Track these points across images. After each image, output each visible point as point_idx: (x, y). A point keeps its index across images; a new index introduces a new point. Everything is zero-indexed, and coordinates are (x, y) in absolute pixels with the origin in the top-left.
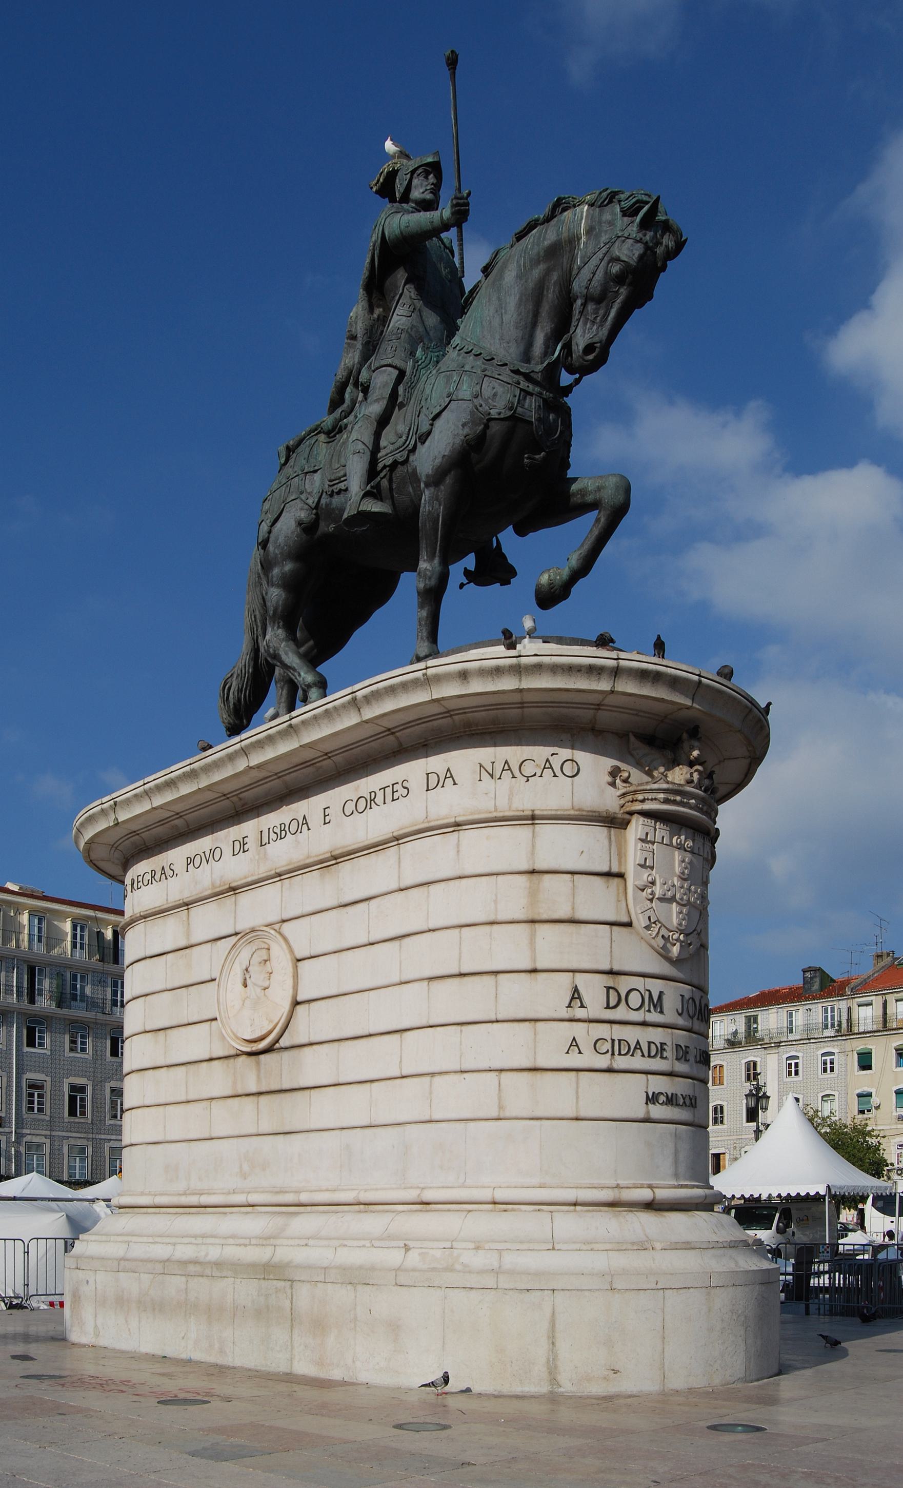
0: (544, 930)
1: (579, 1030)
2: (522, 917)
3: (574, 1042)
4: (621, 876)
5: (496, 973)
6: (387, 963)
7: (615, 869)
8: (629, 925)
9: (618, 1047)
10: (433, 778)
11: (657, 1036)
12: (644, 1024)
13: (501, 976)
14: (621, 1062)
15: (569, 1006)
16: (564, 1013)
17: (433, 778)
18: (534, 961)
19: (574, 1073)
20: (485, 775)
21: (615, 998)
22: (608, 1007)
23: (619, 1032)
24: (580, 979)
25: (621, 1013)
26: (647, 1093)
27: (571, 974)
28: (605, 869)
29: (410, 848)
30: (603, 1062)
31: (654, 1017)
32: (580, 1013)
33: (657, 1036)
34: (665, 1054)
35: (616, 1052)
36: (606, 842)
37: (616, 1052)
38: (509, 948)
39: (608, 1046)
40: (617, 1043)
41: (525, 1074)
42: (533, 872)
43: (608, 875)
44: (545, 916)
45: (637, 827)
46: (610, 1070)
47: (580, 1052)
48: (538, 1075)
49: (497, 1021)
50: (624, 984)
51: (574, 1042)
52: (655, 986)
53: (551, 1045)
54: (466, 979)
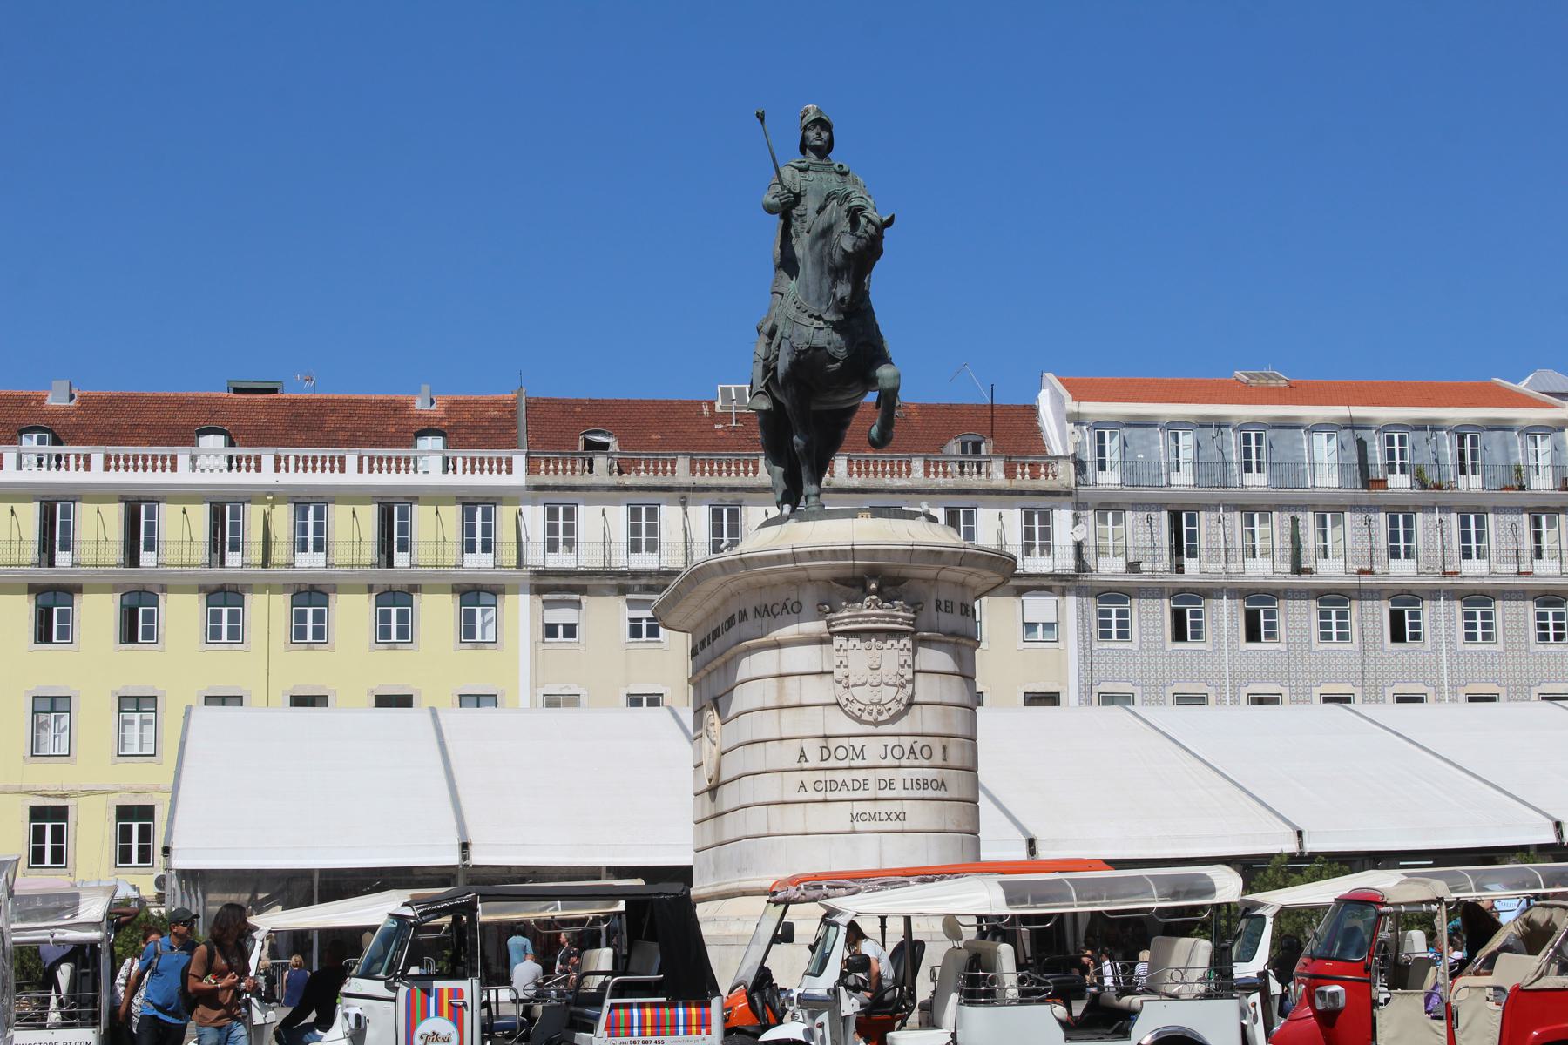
3: (802, 785)
8: (838, 704)
12: (850, 768)
16: (798, 766)
23: (830, 775)
30: (820, 796)
32: (806, 765)
33: (860, 775)
46: (826, 801)
50: (833, 744)
51: (802, 785)
52: (858, 743)
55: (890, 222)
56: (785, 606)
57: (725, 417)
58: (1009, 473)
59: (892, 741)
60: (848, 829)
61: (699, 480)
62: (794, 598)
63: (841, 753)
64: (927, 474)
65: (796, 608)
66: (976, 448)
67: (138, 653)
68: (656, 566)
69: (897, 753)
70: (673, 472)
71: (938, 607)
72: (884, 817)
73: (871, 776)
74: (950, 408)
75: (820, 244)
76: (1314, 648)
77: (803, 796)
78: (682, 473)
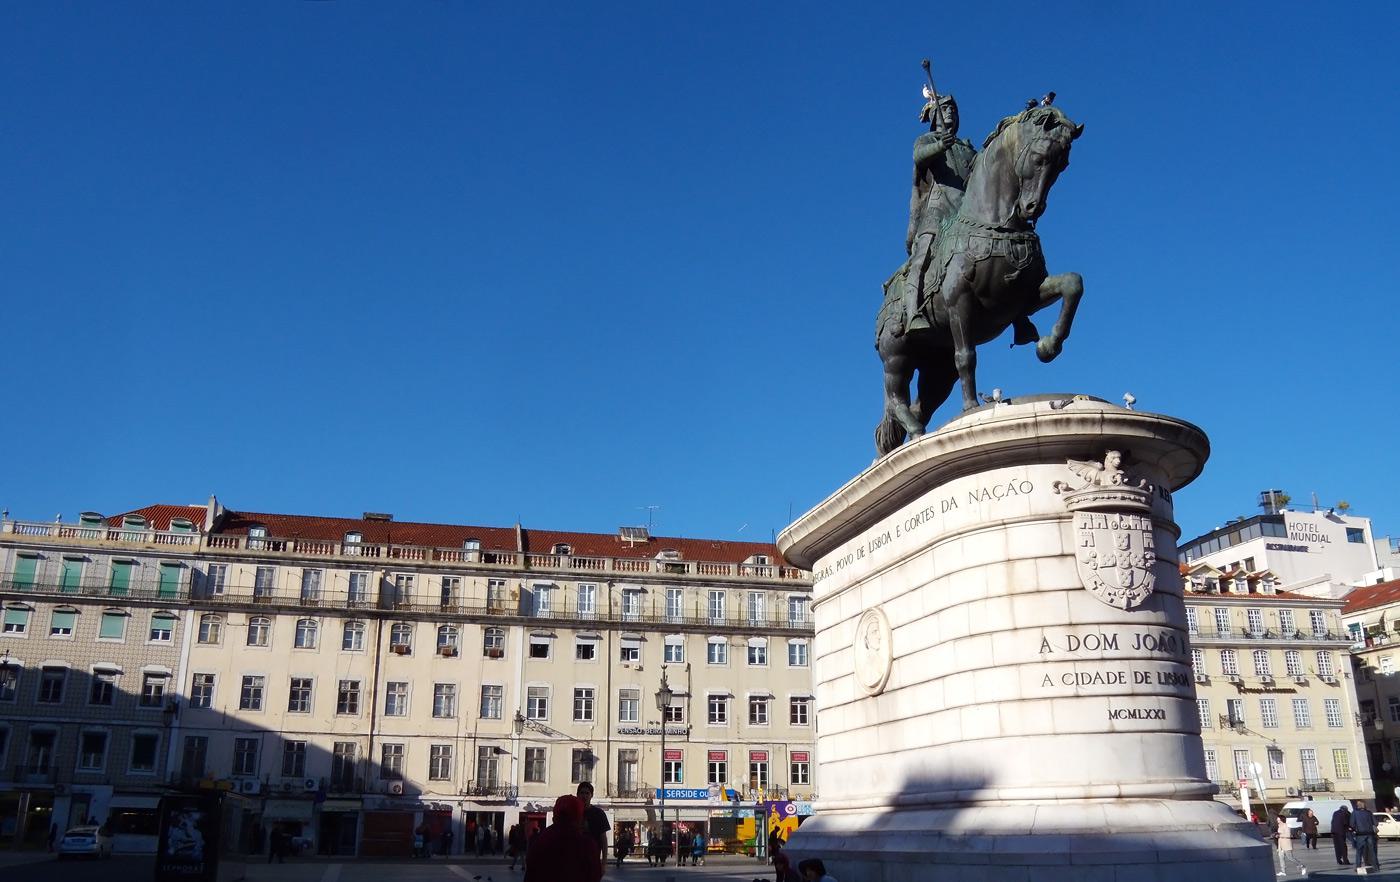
0: (1018, 600)
1: (1050, 669)
2: (1003, 591)
6: (930, 631)
8: (1083, 588)
9: (1079, 679)
10: (945, 504)
13: (995, 635)
14: (1082, 692)
16: (1039, 657)
17: (945, 504)
18: (1014, 622)
19: (1048, 701)
20: (972, 498)
21: (1075, 643)
23: (1080, 668)
24: (1049, 634)
27: (1040, 629)
28: (1059, 553)
29: (939, 550)
30: (1071, 690)
31: (1110, 653)
32: (1050, 657)
34: (1123, 680)
35: (1080, 683)
37: (1080, 683)
38: (997, 615)
40: (1080, 676)
41: (1015, 704)
43: (1063, 555)
44: (1019, 591)
45: (1079, 519)
46: (1078, 696)
48: (1024, 703)
49: (995, 667)
50: (1081, 632)
52: (1109, 631)
53: (1031, 682)
58: (782, 574)
59: (1143, 630)
60: (1106, 729)
61: (617, 572)
63: (1092, 642)
64: (739, 574)
65: (1025, 488)
66: (763, 561)
67: (303, 654)
70: (603, 567)
72: (1144, 714)
74: (743, 544)
75: (997, 163)
77: (1049, 691)
78: (608, 567)
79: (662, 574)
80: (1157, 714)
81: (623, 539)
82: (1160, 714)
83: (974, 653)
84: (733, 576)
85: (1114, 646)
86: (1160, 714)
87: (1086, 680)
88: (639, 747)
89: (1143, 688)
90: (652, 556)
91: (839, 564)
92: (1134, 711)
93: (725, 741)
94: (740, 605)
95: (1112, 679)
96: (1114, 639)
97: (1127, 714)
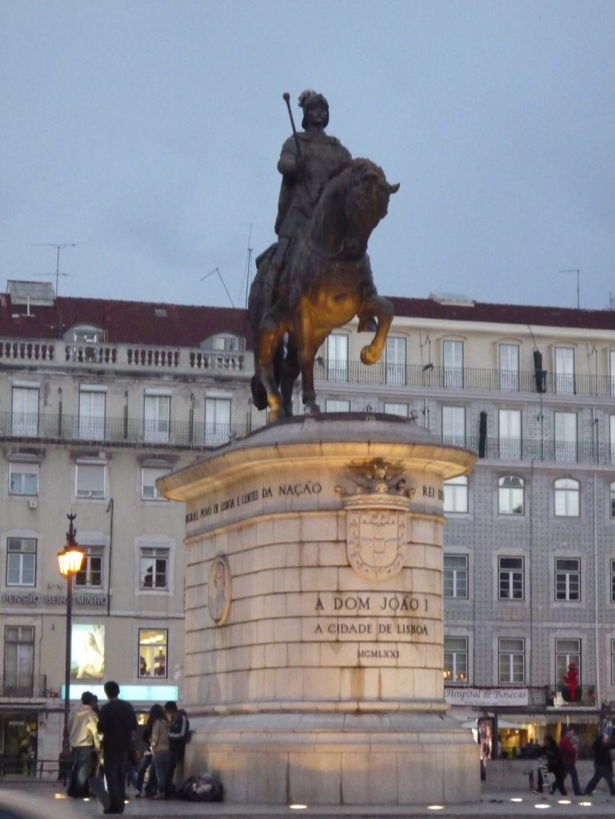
0: (306, 572)
2: (296, 564)
3: (319, 627)
4: (345, 541)
5: (285, 593)
7: (341, 538)
8: (349, 566)
11: (366, 622)
12: (358, 616)
15: (317, 608)
16: (315, 613)
18: (301, 586)
22: (336, 608)
23: (341, 621)
25: (343, 611)
26: (359, 652)
28: (334, 538)
30: (333, 637)
31: (363, 612)
32: (322, 613)
33: (366, 622)
36: (335, 525)
38: (290, 581)
39: (336, 628)
42: (301, 543)
43: (337, 542)
47: (321, 632)
50: (344, 597)
51: (319, 627)
52: (364, 597)
54: (277, 596)
55: (395, 189)
56: (307, 487)
57: (22, 308)
59: (389, 596)
60: (355, 663)
62: (315, 480)
63: (351, 603)
64: (192, 364)
65: (316, 488)
68: (36, 436)
69: (393, 604)
71: (425, 492)
72: (383, 654)
73: (373, 622)
74: (203, 307)
76: (494, 517)
79: (70, 363)
80: (393, 654)
81: (15, 301)
82: (396, 655)
83: (274, 606)
84: (184, 367)
85: (366, 607)
86: (395, 654)
87: (344, 629)
88: (37, 623)
89: (384, 637)
90: (57, 334)
91: (202, 512)
92: (376, 652)
93: (163, 614)
94: (192, 413)
95: (362, 628)
96: (367, 601)
97: (371, 653)
